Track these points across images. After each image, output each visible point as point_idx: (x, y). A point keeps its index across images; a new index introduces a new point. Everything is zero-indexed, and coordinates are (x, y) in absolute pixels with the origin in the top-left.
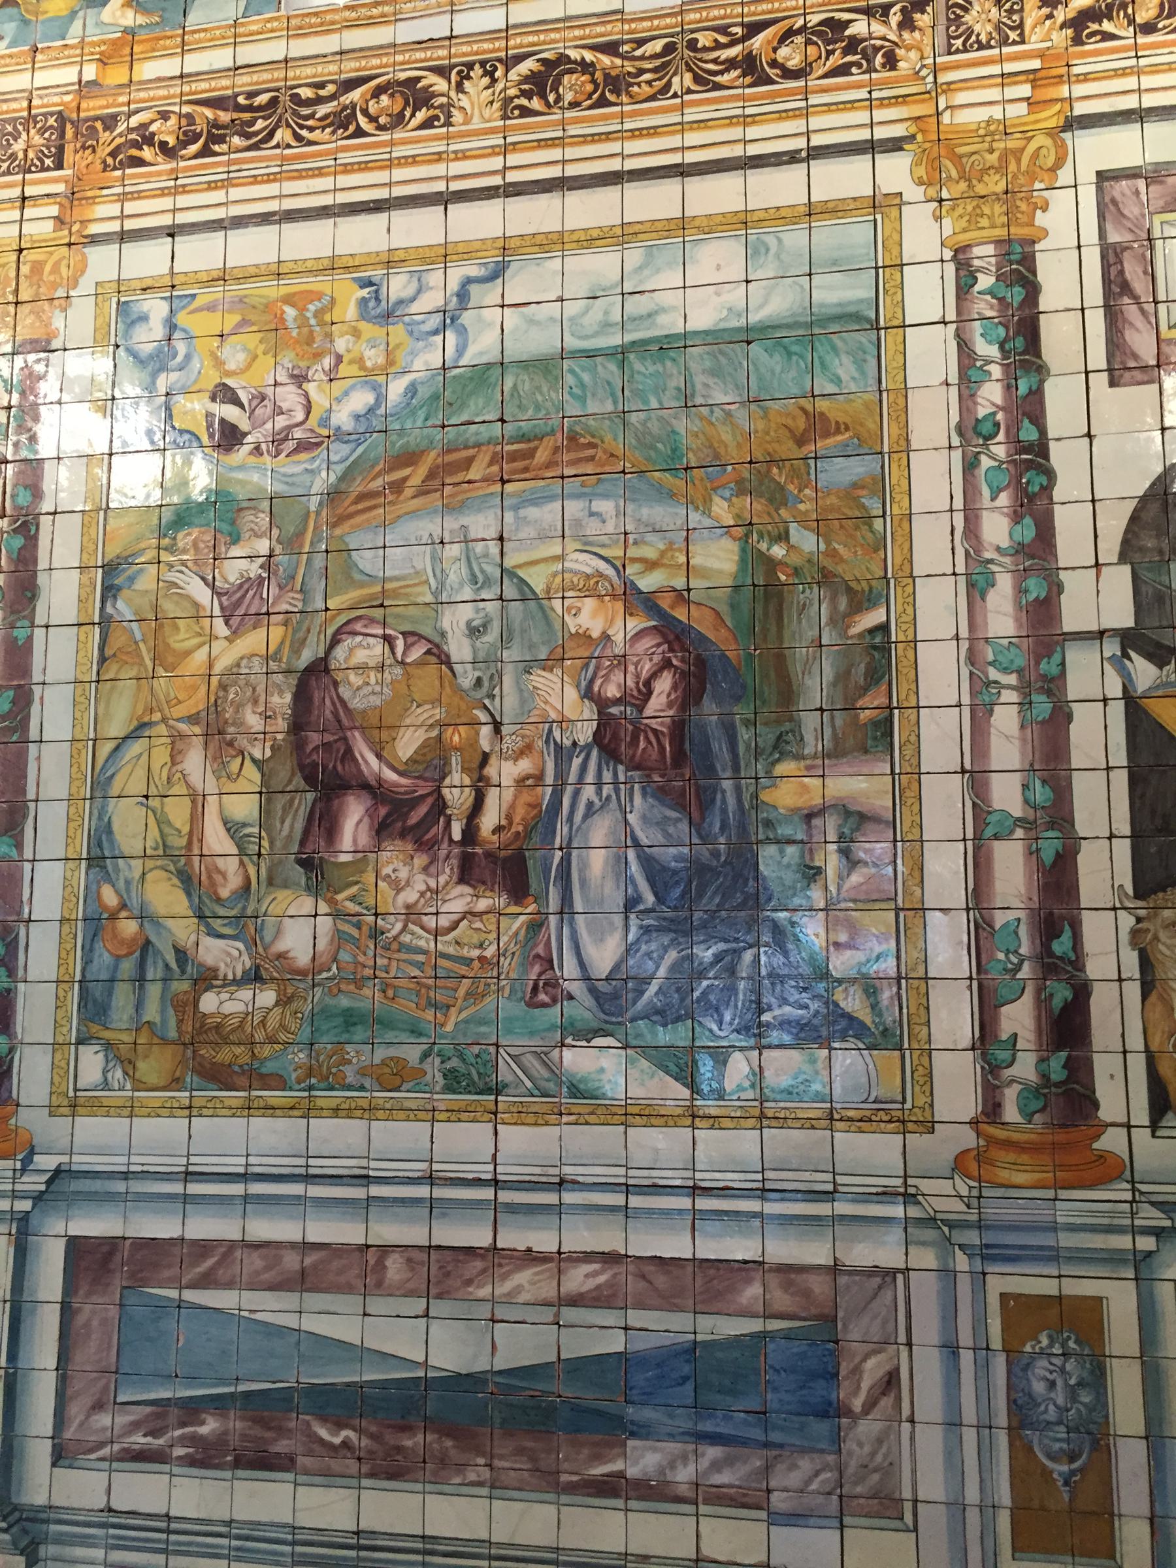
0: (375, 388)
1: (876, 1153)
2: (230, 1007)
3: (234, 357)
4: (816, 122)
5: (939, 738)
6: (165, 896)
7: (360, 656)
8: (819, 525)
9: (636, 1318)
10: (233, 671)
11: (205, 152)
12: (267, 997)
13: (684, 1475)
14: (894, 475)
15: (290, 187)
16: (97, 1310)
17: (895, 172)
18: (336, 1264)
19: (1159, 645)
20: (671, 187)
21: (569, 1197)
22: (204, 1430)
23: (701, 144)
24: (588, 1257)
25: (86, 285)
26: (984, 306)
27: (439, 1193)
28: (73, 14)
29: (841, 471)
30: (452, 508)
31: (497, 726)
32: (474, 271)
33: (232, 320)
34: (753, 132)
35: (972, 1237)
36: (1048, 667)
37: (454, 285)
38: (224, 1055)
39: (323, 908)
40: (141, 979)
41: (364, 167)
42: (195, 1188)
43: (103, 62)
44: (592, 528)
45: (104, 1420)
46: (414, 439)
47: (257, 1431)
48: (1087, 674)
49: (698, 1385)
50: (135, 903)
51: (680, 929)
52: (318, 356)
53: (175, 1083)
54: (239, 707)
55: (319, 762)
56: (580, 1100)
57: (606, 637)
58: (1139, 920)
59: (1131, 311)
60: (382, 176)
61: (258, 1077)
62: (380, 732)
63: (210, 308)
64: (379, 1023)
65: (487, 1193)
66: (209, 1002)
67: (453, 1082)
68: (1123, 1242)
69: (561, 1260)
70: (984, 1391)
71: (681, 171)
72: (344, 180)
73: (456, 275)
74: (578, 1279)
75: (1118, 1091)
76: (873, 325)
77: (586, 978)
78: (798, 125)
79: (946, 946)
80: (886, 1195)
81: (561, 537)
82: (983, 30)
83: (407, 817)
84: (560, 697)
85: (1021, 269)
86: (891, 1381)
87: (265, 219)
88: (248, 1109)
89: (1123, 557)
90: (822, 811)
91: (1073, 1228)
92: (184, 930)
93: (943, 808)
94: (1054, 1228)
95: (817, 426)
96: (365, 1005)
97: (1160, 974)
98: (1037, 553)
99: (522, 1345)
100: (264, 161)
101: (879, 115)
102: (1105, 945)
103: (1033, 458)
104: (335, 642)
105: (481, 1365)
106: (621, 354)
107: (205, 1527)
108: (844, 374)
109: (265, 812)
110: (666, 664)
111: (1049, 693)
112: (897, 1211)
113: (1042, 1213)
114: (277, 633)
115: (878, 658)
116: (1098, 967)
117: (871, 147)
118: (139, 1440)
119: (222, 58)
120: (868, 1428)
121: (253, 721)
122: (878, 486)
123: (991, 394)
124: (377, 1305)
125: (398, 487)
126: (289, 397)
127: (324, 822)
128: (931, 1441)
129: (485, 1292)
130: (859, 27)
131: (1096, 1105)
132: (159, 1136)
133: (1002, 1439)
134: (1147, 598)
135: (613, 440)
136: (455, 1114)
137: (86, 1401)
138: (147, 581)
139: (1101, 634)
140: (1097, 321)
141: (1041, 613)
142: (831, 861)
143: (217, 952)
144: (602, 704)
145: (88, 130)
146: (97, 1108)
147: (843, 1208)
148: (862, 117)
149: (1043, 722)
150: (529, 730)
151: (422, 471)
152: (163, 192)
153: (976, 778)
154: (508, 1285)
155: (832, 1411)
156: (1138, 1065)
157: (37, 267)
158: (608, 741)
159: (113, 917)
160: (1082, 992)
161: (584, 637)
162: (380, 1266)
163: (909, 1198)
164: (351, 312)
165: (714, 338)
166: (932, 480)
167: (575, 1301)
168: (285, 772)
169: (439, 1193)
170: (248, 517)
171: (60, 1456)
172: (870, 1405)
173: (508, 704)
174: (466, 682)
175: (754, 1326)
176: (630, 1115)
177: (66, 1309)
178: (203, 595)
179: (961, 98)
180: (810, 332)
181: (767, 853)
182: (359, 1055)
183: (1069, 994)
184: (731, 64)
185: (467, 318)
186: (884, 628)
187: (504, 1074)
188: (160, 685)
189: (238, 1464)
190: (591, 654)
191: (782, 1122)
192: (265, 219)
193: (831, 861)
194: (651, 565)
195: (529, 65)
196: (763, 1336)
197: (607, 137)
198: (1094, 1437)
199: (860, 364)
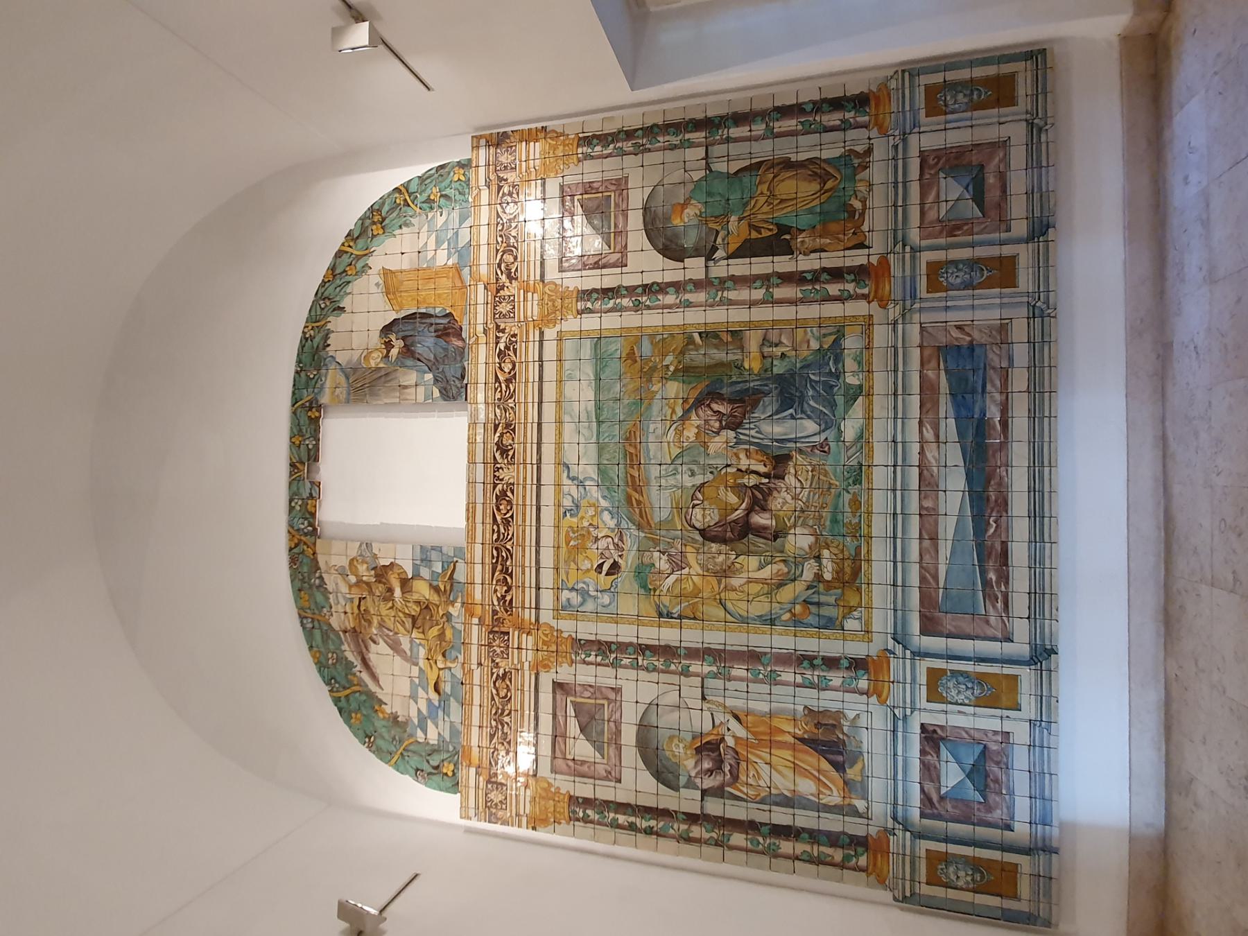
0: (602, 511)
1: (881, 335)
2: (830, 569)
3: (586, 565)
4: (531, 359)
5: (738, 315)
6: (787, 594)
7: (699, 517)
8: (664, 355)
9: (942, 414)
10: (702, 566)
11: (511, 575)
12: (826, 553)
13: (997, 396)
14: (650, 331)
15: (527, 543)
16: (948, 623)
17: (550, 333)
18: (927, 525)
20: (545, 405)
21: (899, 439)
22: (994, 578)
23: (533, 395)
24: (921, 432)
25: (553, 623)
26: (597, 305)
27: (899, 487)
28: (453, 627)
29: (646, 348)
30: (648, 484)
31: (728, 466)
32: (565, 474)
33: (573, 566)
34: (531, 380)
35: (908, 303)
36: (716, 282)
37: (570, 482)
38: (848, 570)
39: (792, 531)
40: (818, 604)
41: (524, 514)
42: (899, 583)
43: (472, 616)
44: (659, 432)
45: (992, 620)
46: (622, 497)
47: (993, 557)
48: (719, 270)
49: (965, 394)
50: (788, 606)
51: (802, 399)
52: (589, 533)
53: (859, 590)
54: (716, 564)
55: (736, 533)
56: (863, 438)
57: (698, 427)
59: (604, 261)
60: (528, 508)
61: (856, 558)
62: (727, 509)
63: (567, 574)
64: (834, 513)
65: (899, 469)
66: (828, 576)
67: (857, 481)
68: (908, 256)
69: (922, 442)
70: (962, 298)
71: (540, 403)
72: (528, 523)
73: (566, 481)
74: (929, 435)
75: (857, 258)
76: (599, 339)
77: (819, 433)
78: (531, 365)
79: (810, 312)
80: (895, 330)
81: (660, 442)
82: (509, 307)
83: (759, 499)
84: (717, 444)
85: (586, 294)
86: (959, 328)
87: (537, 552)
88: (869, 561)
90: (762, 353)
91: (904, 271)
92: (800, 586)
93: (763, 314)
94: (904, 277)
95: (631, 356)
96: (829, 516)
98: (678, 286)
99: (954, 455)
100: (517, 552)
101: (531, 339)
102: (808, 263)
103: (647, 289)
104: (694, 527)
105: (962, 470)
106: (599, 423)
107: (1033, 578)
108: (616, 348)
109: (755, 554)
110: (709, 406)
112: (900, 327)
113: (900, 281)
114: (689, 549)
115: (710, 335)
116: (816, 265)
117: (541, 342)
118: (999, 605)
119: (478, 568)
120: (976, 335)
121: (721, 558)
122: (652, 336)
123: (626, 302)
124: (942, 511)
125: (639, 502)
126: (602, 544)
127: (760, 531)
128: (979, 315)
129: (935, 469)
130: (502, 346)
132: (880, 596)
133: (977, 292)
134: (696, 253)
135: (628, 426)
136: (870, 480)
137: (986, 628)
138: (666, 600)
140: (605, 271)
141: (698, 285)
142: (778, 351)
143: (808, 575)
144: (722, 428)
145: (498, 621)
146: (868, 622)
147: (900, 345)
148: (531, 344)
150: (730, 454)
151: (634, 494)
152: (523, 592)
153: (752, 304)
154: (933, 461)
155: (971, 347)
156: (848, 253)
157: (544, 643)
158: (735, 425)
159: (794, 615)
160: (824, 270)
161: (697, 435)
162: (927, 509)
163: (895, 323)
164: (575, 520)
165: (598, 390)
166: (652, 319)
167: (937, 436)
168: (741, 546)
169: (899, 487)
170: (645, 560)
171: (1009, 640)
172: (969, 335)
173: (720, 462)
174: (711, 477)
175: (943, 373)
176: (869, 418)
177: (949, 636)
178: (673, 578)
179: (529, 314)
180: (600, 360)
181: (775, 370)
182: (848, 517)
184: (507, 387)
185: (581, 478)
186: (700, 333)
187: (855, 463)
188: (705, 595)
189: (1007, 565)
190: (704, 434)
191: (870, 364)
192: (537, 552)
193: (778, 351)
194: (674, 412)
195: (498, 455)
196: (946, 371)
197: (525, 428)
198: (973, 263)
199: (611, 343)
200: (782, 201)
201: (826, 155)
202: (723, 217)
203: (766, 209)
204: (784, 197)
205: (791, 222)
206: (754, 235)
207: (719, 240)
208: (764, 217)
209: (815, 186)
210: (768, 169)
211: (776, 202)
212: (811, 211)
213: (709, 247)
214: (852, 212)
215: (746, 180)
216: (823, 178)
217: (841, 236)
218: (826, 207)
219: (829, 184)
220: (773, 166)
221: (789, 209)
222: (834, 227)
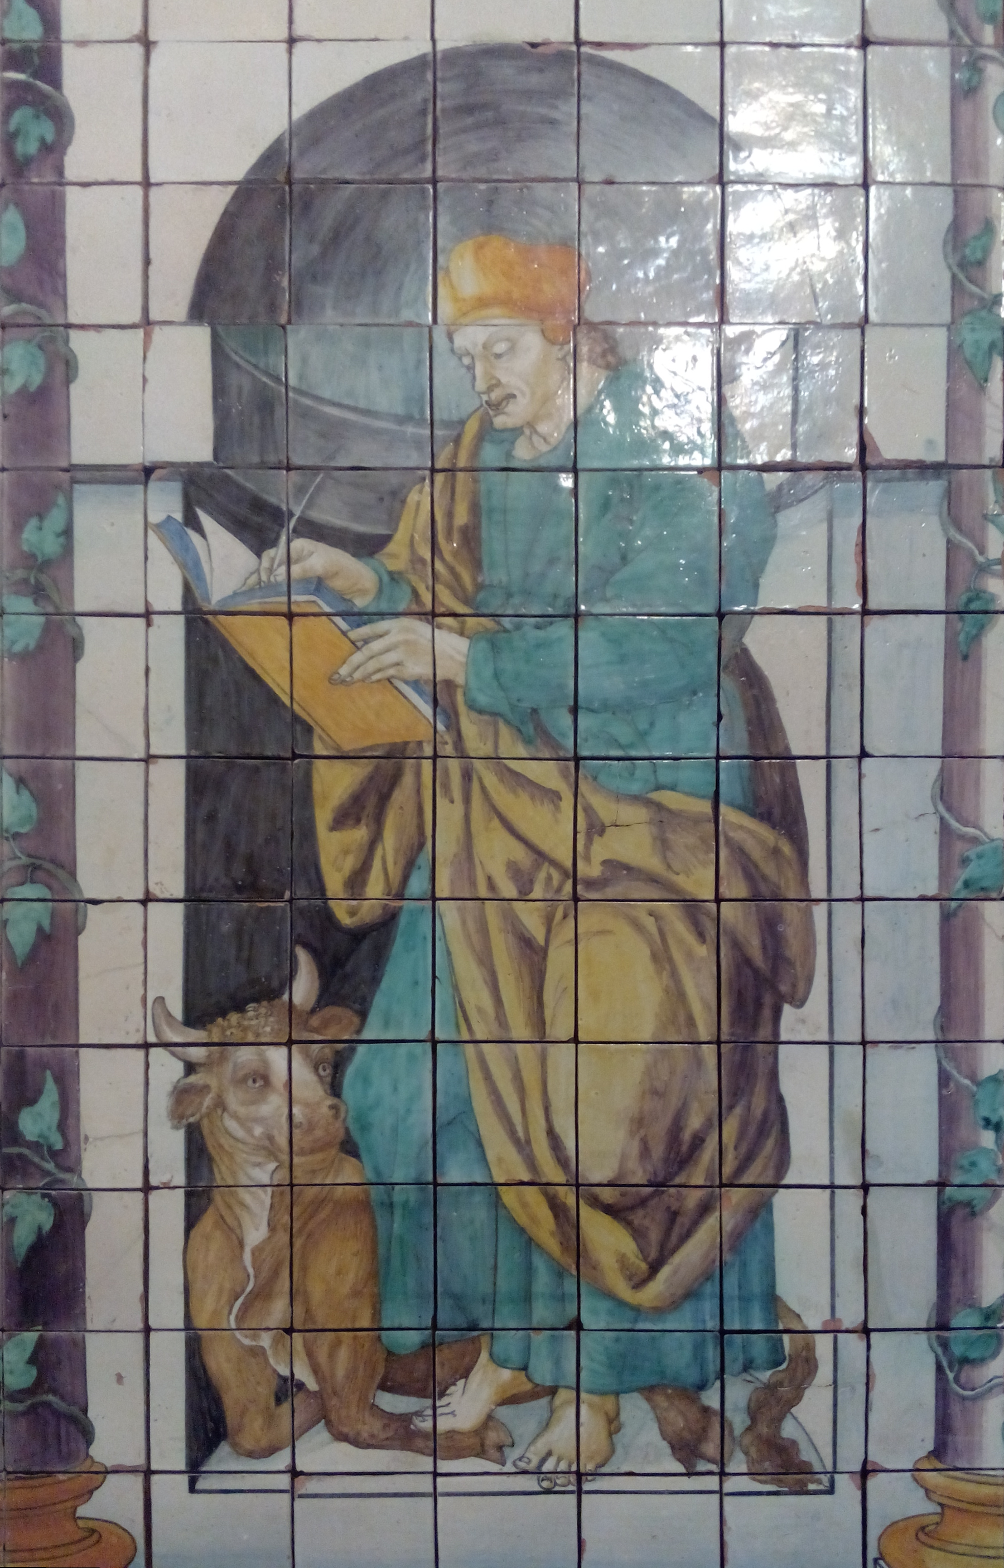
19: (259, 505)
36: (40, 538)
58: (190, 1068)
89: (200, 309)
97: (222, 1174)
111: (38, 593)
116: (106, 1161)
131: (87, 1434)
139: (148, 471)
149: (24, 658)
156: (170, 1353)
183: (46, 1219)
200: (533, 955)
201: (798, 1223)
202: (461, 584)
203: (496, 853)
204: (559, 960)
205: (398, 998)
206: (334, 784)
207: (317, 558)
208: (447, 843)
209: (606, 1150)
210: (750, 871)
211: (531, 918)
212: (450, 1124)
213: (280, 490)
214: (424, 1374)
215: (692, 728)
216: (654, 1201)
217: (278, 1311)
218: (467, 1220)
219: (607, 1240)
220: (763, 896)
221: (477, 996)
222: (336, 1268)
